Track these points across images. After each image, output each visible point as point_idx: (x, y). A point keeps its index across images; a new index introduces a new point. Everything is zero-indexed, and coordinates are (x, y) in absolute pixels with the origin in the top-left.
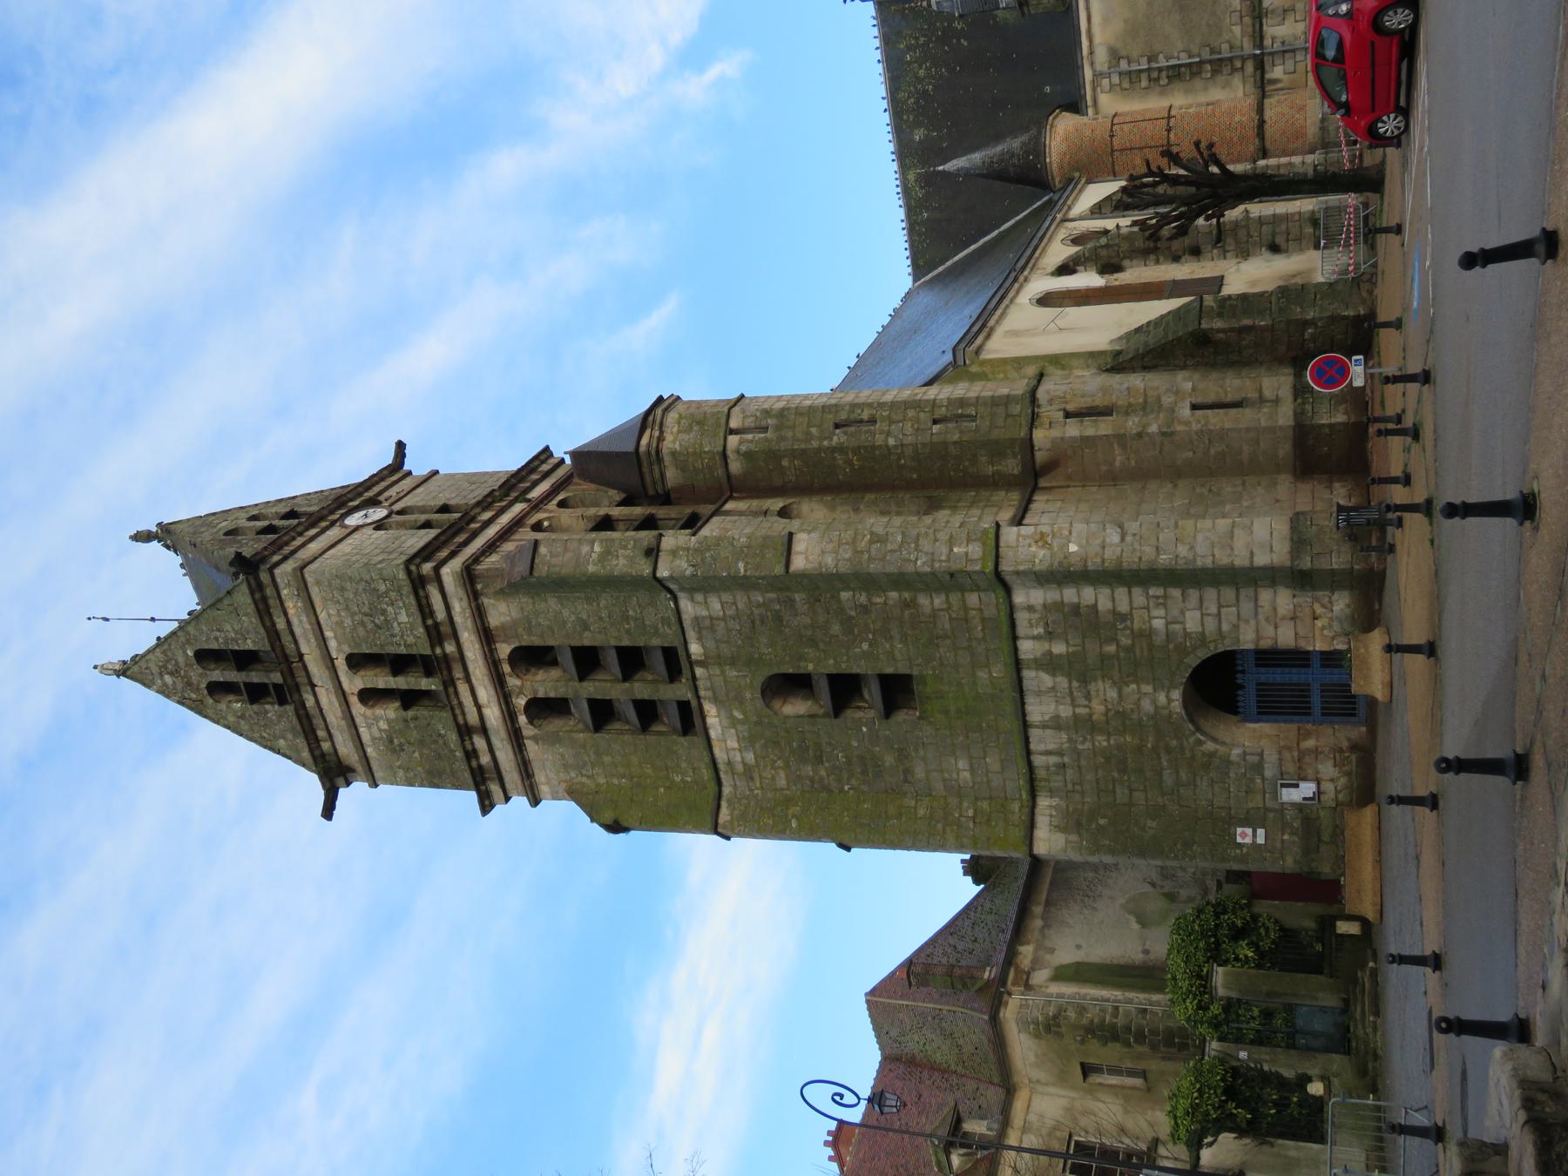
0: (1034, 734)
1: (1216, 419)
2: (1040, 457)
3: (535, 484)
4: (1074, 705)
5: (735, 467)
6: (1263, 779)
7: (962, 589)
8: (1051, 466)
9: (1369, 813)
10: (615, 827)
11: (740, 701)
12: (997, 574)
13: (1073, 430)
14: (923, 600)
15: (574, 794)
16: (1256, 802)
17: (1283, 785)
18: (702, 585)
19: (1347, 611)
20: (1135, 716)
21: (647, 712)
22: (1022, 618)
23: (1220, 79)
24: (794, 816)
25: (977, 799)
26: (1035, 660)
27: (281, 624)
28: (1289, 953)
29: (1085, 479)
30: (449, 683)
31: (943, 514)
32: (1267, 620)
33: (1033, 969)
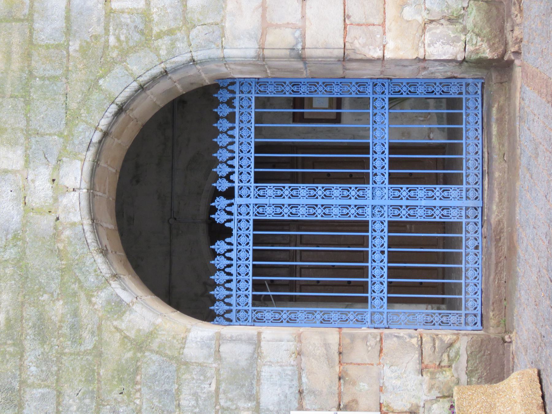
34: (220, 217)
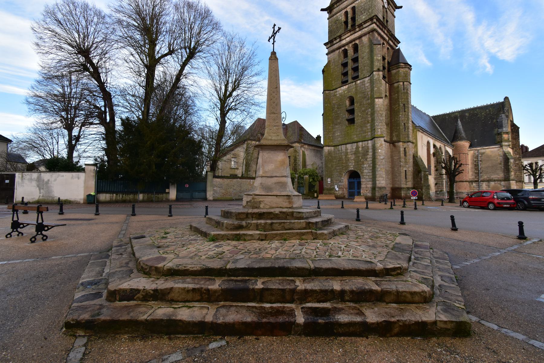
0: (345, 146)
1: (403, 175)
2: (397, 144)
3: (392, 41)
5: (396, 85)
7: (371, 131)
8: (394, 146)
9: (334, 198)
10: (323, 71)
11: (349, 92)
12: (375, 138)
13: (402, 149)
15: (329, 62)
16: (335, 181)
18: (372, 82)
21: (345, 74)
22: (366, 142)
23: (474, 174)
28: (311, 187)
29: (392, 152)
30: (350, 31)
31: (385, 127)
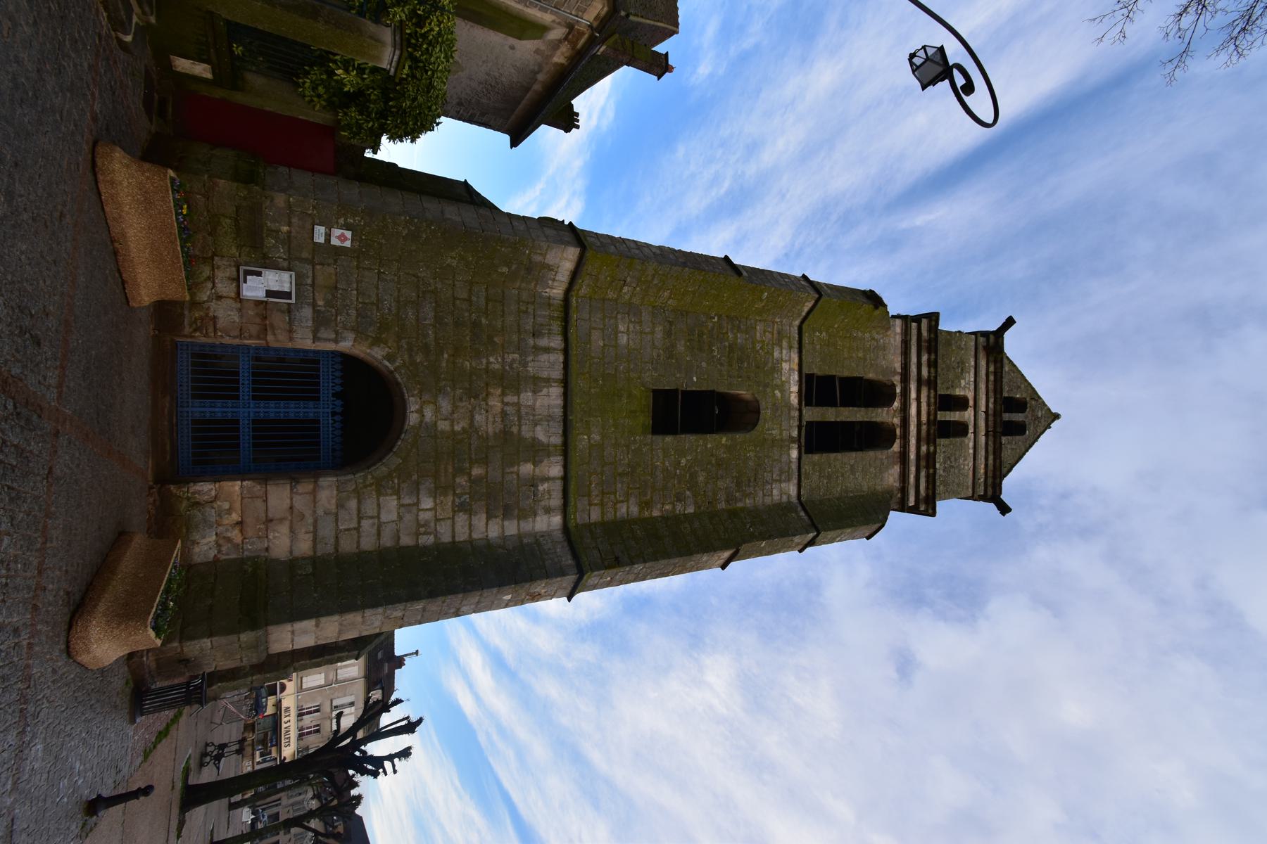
0: (557, 373)
4: (518, 404)
6: (314, 305)
11: (775, 407)
14: (635, 510)
16: (326, 274)
17: (287, 295)
19: (196, 536)
20: (459, 392)
22: (556, 501)
24: (762, 300)
25: (616, 300)
26: (549, 456)
27: (991, 458)
32: (302, 517)
33: (560, 41)
34: (339, 402)
